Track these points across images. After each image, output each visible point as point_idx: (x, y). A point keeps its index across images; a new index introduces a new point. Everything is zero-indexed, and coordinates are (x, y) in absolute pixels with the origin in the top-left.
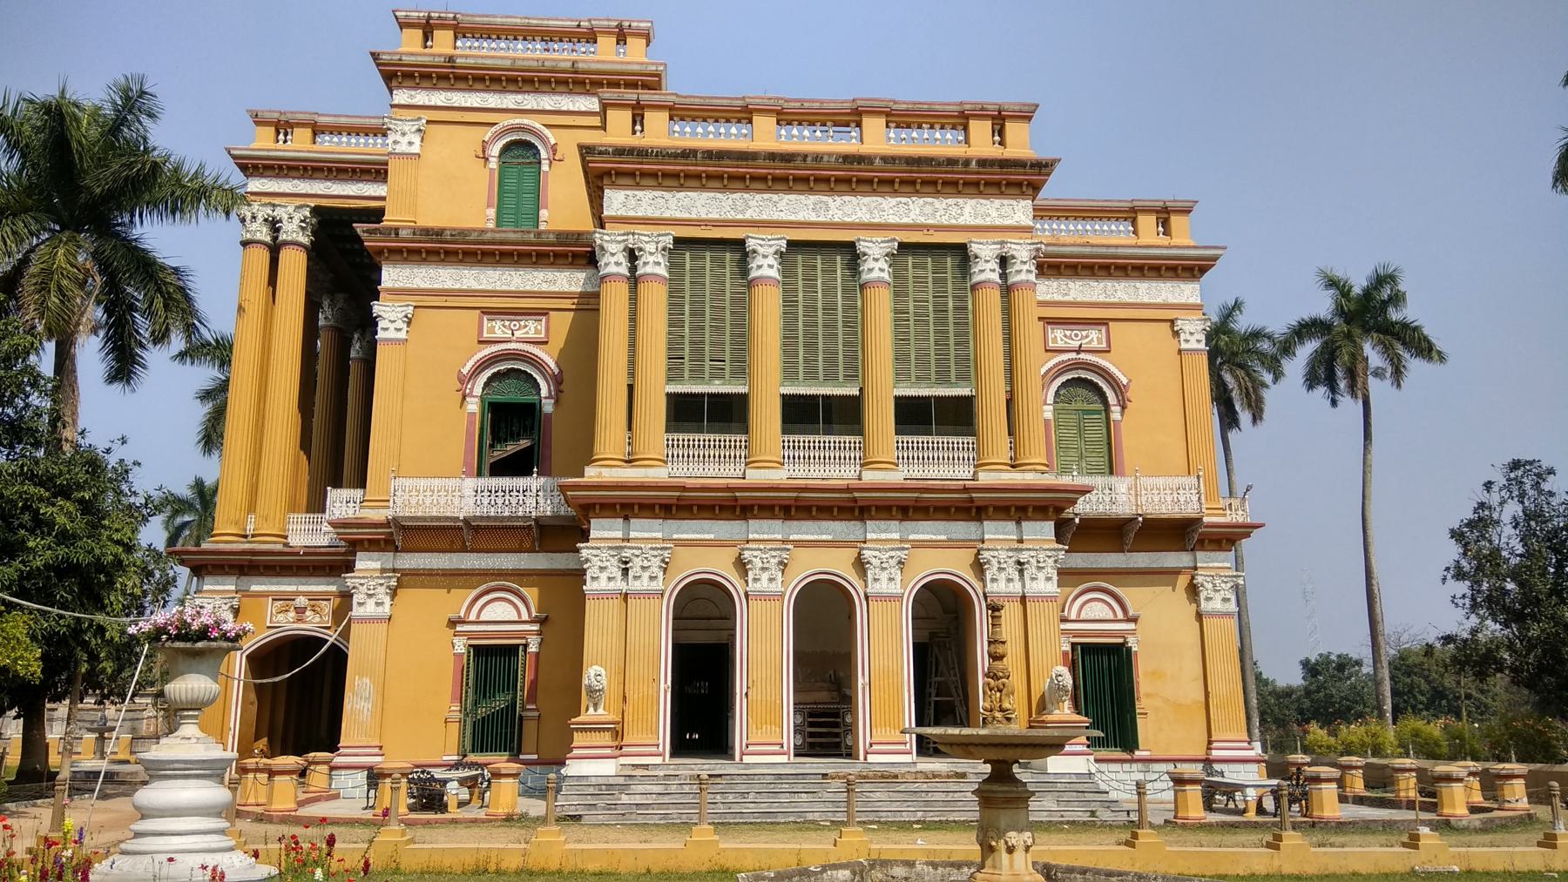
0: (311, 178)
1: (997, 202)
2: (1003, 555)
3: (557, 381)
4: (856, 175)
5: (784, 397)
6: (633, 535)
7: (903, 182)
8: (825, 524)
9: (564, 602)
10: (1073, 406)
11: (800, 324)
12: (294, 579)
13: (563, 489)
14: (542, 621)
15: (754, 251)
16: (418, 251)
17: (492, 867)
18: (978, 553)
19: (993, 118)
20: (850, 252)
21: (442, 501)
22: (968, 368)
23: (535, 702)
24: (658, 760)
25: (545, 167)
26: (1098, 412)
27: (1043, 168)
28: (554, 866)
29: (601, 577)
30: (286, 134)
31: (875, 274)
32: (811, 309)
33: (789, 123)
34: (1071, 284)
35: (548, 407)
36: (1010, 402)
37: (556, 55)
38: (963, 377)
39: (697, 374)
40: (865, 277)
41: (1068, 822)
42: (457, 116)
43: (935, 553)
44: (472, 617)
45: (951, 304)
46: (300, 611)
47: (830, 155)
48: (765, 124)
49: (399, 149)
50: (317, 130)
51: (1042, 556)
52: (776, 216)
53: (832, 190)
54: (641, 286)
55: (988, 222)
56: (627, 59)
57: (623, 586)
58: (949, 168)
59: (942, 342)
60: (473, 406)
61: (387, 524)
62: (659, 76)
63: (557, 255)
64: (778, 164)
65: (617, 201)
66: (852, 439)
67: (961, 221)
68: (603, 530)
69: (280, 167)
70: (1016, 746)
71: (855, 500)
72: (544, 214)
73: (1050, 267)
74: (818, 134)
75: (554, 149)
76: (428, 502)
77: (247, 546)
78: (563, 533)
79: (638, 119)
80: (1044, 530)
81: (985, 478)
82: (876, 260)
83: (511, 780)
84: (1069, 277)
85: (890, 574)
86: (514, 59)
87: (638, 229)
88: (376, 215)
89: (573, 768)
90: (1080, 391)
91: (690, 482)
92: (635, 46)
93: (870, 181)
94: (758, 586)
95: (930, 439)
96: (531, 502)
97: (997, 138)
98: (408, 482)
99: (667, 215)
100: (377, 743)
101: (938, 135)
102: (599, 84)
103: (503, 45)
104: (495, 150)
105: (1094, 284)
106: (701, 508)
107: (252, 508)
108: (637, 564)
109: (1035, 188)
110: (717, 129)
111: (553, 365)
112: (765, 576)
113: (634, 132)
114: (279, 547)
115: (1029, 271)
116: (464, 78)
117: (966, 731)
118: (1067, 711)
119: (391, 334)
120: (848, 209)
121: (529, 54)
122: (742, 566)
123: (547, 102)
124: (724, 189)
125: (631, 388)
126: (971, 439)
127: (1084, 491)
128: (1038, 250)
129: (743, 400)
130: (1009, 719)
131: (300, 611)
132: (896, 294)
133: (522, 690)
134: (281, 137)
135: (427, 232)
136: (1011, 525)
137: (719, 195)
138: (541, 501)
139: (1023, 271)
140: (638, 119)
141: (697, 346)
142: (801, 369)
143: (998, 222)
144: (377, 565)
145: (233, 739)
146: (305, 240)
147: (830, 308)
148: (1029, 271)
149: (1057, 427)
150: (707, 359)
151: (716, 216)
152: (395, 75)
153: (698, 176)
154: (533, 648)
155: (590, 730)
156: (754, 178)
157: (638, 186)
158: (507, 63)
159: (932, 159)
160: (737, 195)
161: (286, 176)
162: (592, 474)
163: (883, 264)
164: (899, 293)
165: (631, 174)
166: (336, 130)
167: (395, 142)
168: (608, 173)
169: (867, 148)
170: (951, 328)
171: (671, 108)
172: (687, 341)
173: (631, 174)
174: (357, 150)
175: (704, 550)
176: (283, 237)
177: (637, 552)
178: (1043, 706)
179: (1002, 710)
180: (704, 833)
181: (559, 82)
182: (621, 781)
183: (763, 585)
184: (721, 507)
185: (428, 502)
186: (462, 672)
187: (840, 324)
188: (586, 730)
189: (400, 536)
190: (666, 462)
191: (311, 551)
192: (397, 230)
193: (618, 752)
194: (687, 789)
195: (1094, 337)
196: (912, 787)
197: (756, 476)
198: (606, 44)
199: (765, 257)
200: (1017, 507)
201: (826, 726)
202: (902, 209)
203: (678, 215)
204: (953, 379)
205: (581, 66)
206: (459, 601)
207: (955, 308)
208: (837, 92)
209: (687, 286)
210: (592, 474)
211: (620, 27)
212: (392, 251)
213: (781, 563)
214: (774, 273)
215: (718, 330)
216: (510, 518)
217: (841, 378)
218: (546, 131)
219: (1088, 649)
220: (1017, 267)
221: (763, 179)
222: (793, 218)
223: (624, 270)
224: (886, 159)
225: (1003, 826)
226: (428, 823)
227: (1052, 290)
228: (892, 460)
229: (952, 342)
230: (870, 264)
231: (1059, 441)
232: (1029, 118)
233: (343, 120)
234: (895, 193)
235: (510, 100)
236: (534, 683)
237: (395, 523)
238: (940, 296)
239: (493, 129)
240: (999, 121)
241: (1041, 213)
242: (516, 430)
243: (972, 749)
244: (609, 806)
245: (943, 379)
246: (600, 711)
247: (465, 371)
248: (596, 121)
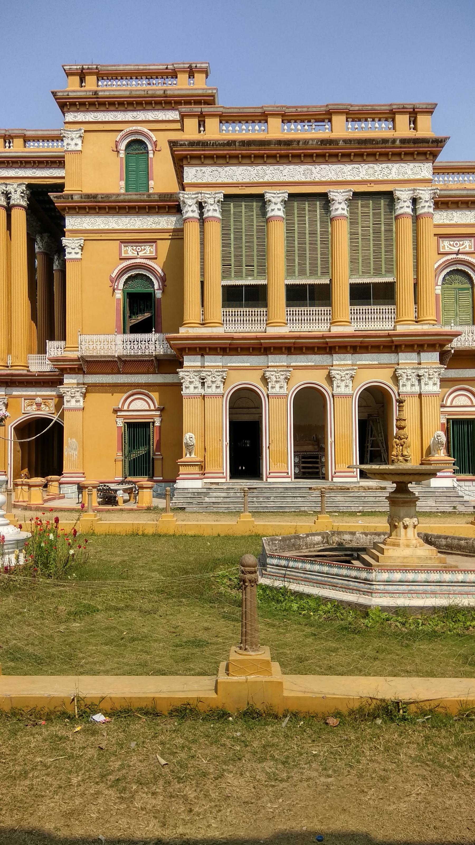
0: (25, 167)
1: (412, 165)
2: (409, 372)
3: (163, 280)
4: (329, 152)
5: (287, 286)
6: (206, 364)
7: (356, 155)
8: (310, 357)
9: (172, 400)
10: (453, 286)
11: (296, 243)
12: (34, 389)
13: (168, 340)
14: (162, 410)
15: (270, 201)
16: (84, 208)
17: (140, 533)
18: (396, 371)
19: (410, 113)
20: (324, 198)
21: (106, 347)
22: (392, 266)
23: (160, 451)
24: (223, 480)
25: (151, 155)
26: (467, 289)
27: (439, 143)
28: (171, 532)
29: (191, 388)
30: (10, 143)
31: (339, 212)
32: (302, 234)
33: (289, 121)
34: (455, 214)
35: (159, 294)
36: (416, 285)
37: (154, 87)
38: (389, 272)
39: (239, 275)
40: (333, 214)
41: (440, 512)
42: (101, 127)
43: (371, 371)
44: (125, 408)
45: (383, 228)
46: (39, 405)
47: (313, 140)
48: (274, 122)
49: (72, 147)
50: (26, 139)
51: (431, 372)
52: (282, 179)
53: (314, 162)
54: (206, 224)
55: (406, 177)
56: (195, 87)
57: (200, 391)
58: (383, 145)
59: (377, 252)
60: (119, 295)
61: (78, 360)
62: (213, 96)
63: (160, 207)
64: (282, 147)
65: (191, 174)
66: (326, 308)
67: (390, 177)
68: (190, 362)
69: (8, 162)
70: (410, 474)
71: (327, 343)
72: (151, 183)
73: (442, 203)
74: (306, 127)
75: (155, 144)
76: (98, 347)
77: (9, 372)
78: (169, 363)
79: (201, 123)
80: (432, 358)
81: (401, 329)
82: (340, 203)
83: (149, 490)
84: (453, 209)
85: (346, 381)
86: (131, 91)
87: (204, 190)
88: (60, 187)
89: (180, 484)
90: (457, 277)
91: (236, 335)
92: (199, 77)
93: (336, 155)
94: (274, 391)
95: (370, 307)
96: (152, 347)
97: (412, 125)
98: (88, 337)
99: (220, 181)
100: (82, 471)
101: (377, 125)
102: (179, 103)
103: (124, 82)
104: (123, 146)
105: (468, 213)
106: (242, 349)
107: (9, 352)
108: (209, 379)
109: (435, 155)
110: (247, 127)
111: (160, 271)
112: (278, 385)
113: (200, 132)
114: (25, 372)
115: (429, 207)
116: (103, 104)
117: (383, 467)
118: (442, 455)
119: (73, 256)
120: (324, 173)
121: (139, 87)
122: (265, 380)
123: (150, 115)
124: (252, 164)
125: (202, 283)
126: (393, 307)
127: (457, 335)
128: (435, 193)
129: (264, 288)
130: (406, 461)
131: (39, 405)
132: (351, 223)
133: (153, 445)
134: (7, 144)
135: (88, 196)
136: (414, 355)
137: (249, 168)
138: (158, 346)
139: (426, 207)
140: (201, 123)
141: (238, 257)
142: (297, 269)
143: (412, 177)
144: (75, 381)
145: (10, 471)
146: (24, 204)
147: (313, 233)
148: (429, 207)
149: (443, 298)
150: (244, 265)
151: (248, 181)
152: (66, 104)
153: (236, 157)
154: (157, 424)
155: (188, 465)
156: (269, 156)
157: (203, 164)
158: (127, 93)
159: (373, 140)
160: (259, 168)
161: (11, 167)
162: (183, 331)
163: (344, 206)
164: (353, 223)
165: (198, 157)
166: (36, 139)
167: (68, 144)
168: (185, 157)
169: (335, 135)
170: (383, 242)
171: (220, 116)
172: (232, 255)
173: (198, 157)
174: (48, 150)
175: (244, 372)
176: (12, 202)
177: (209, 373)
178: (429, 452)
179: (402, 456)
180: (247, 517)
181: (157, 103)
182: (205, 490)
183: (277, 390)
184: (253, 349)
185: (98, 347)
186: (122, 436)
187: (319, 242)
188: (186, 465)
189: (86, 365)
190: (223, 324)
191: (41, 374)
192: (72, 196)
193: (203, 476)
194: (238, 495)
196: (357, 494)
197: (272, 331)
198: (183, 77)
199: (276, 204)
200: (418, 345)
201: (311, 463)
202: (355, 171)
203: (226, 181)
204: (383, 273)
205: (169, 92)
206: (118, 399)
207: (385, 230)
208: (317, 101)
209: (232, 223)
210: (183, 331)
211: (190, 67)
212: (71, 208)
213: (286, 378)
214: (281, 213)
215: (250, 248)
216: (142, 356)
217: (319, 274)
218: (151, 133)
219: (456, 422)
220: (422, 204)
221: (274, 157)
222: (291, 180)
223: (196, 215)
224: (346, 141)
225: (402, 515)
226: (108, 511)
227: (444, 217)
228: (347, 320)
229: (383, 250)
230: (336, 206)
231: (444, 306)
232: (431, 113)
233: (40, 133)
234: (352, 162)
235: (129, 116)
236: (159, 442)
237: (82, 358)
238: (377, 223)
239: (121, 134)
240: (413, 114)
241: (437, 171)
242: (143, 307)
243: (386, 476)
244: (199, 503)
245: (377, 272)
246: (193, 456)
247: (113, 276)
248: (178, 126)
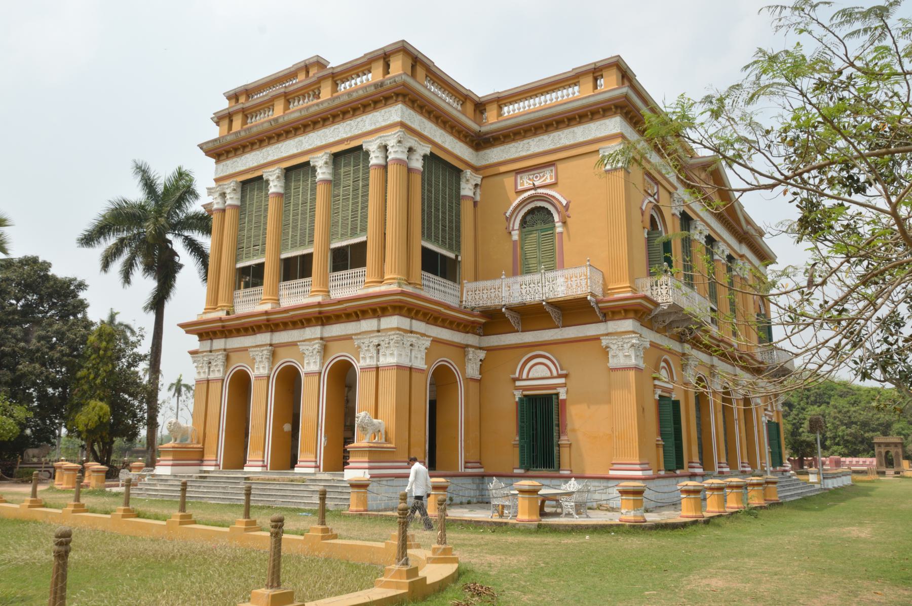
108: (214, 364)
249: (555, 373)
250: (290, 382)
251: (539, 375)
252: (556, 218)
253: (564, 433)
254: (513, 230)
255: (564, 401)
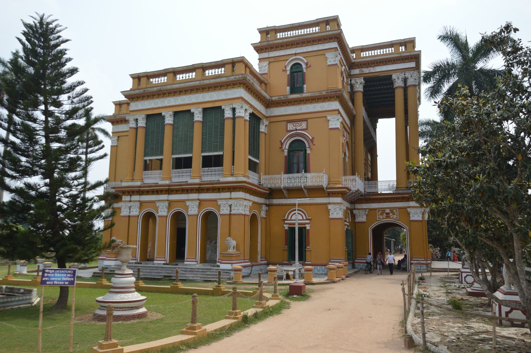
29: (125, 212)
195: (304, 125)
249: (305, 218)
250: (179, 219)
251: (297, 218)
252: (307, 146)
253: (309, 245)
254: (285, 149)
255: (308, 230)
